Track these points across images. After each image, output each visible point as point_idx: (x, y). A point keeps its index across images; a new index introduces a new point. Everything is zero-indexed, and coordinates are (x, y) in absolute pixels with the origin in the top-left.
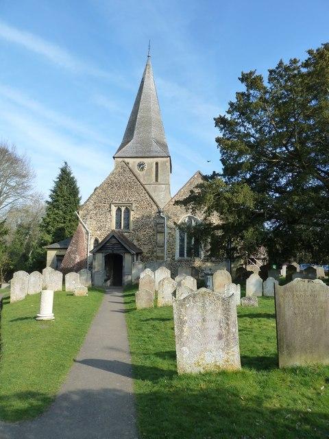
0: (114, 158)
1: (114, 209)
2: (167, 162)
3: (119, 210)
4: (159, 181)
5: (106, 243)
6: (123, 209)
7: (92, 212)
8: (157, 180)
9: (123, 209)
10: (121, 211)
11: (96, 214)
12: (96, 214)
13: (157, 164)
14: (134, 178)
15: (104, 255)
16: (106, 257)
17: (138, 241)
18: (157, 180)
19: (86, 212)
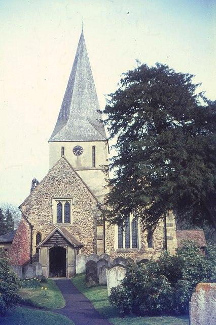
1: (55, 203)
3: (60, 205)
5: (51, 237)
6: (63, 203)
9: (63, 203)
10: (62, 205)
13: (94, 147)
15: (48, 248)
16: (50, 250)
17: (79, 233)
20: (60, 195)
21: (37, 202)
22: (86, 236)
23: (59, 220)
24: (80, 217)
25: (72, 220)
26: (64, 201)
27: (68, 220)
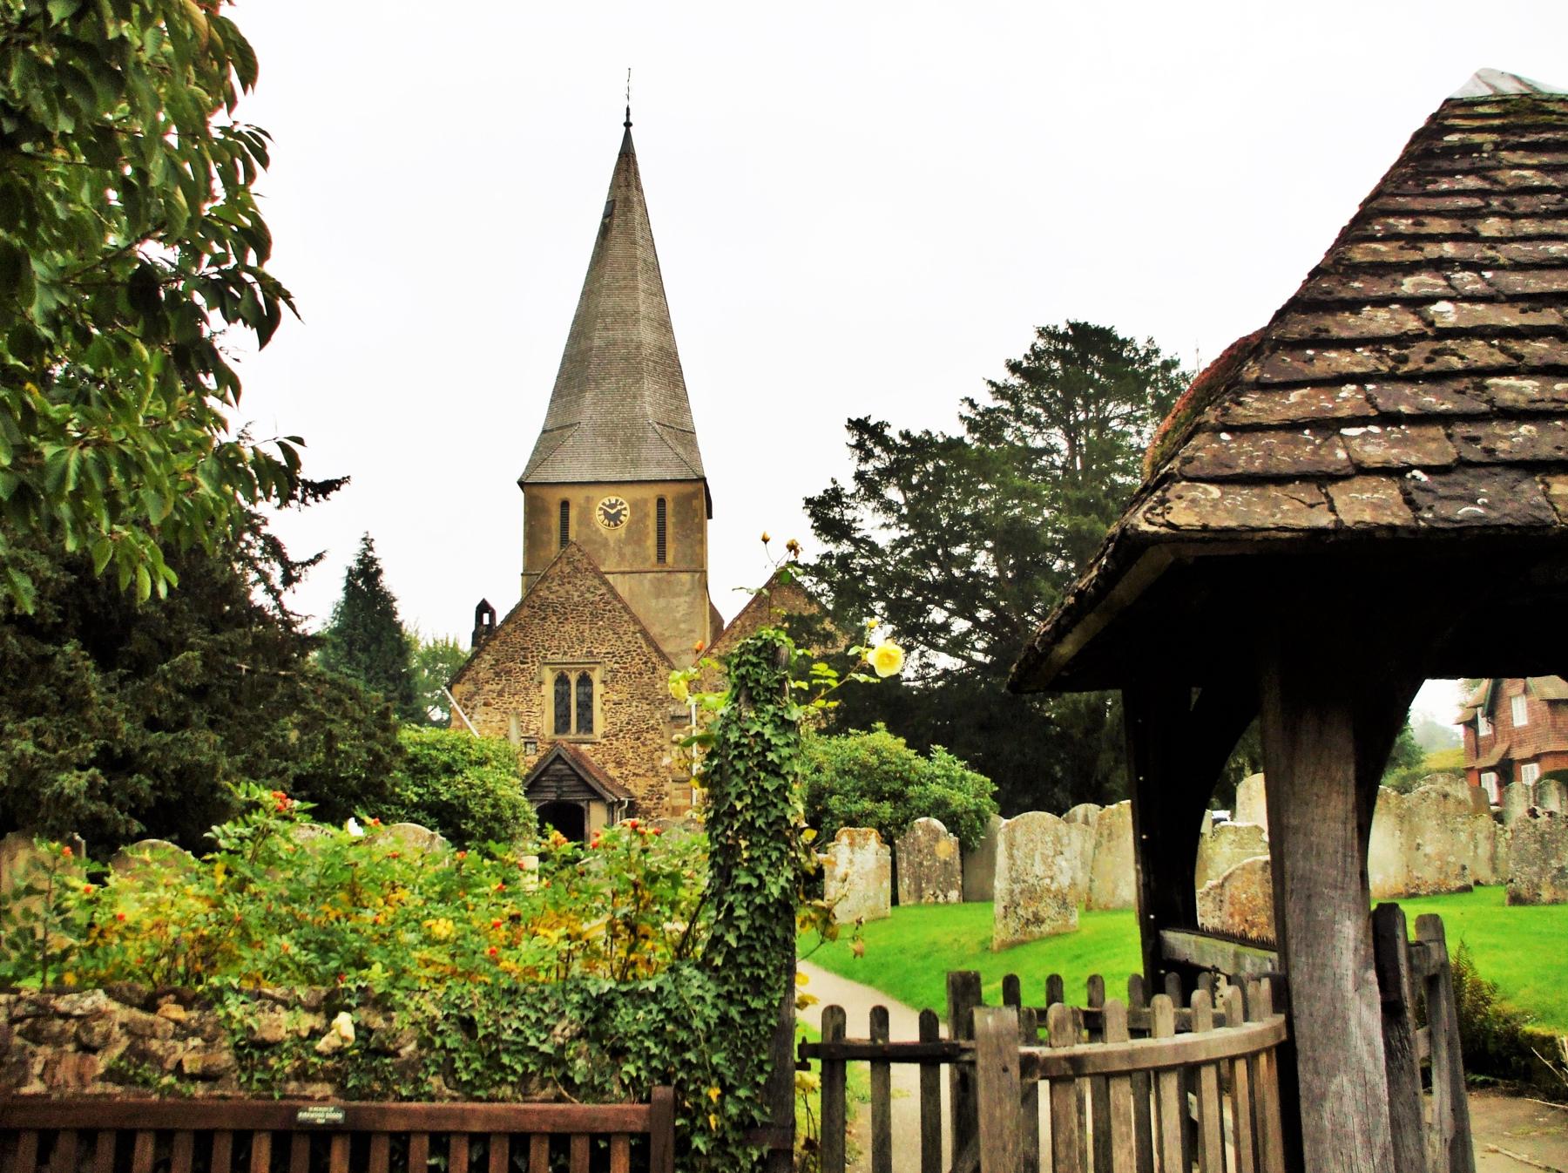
0: (521, 484)
1: (549, 676)
2: (694, 496)
3: (562, 680)
4: (669, 558)
5: (542, 774)
6: (573, 678)
7: (487, 687)
8: (661, 556)
9: (573, 678)
10: (568, 683)
11: (500, 694)
12: (500, 694)
13: (661, 502)
14: (603, 590)
17: (619, 764)
18: (661, 556)
19: (473, 689)
20: (565, 653)
21: (497, 674)
22: (641, 771)
23: (562, 724)
24: (625, 718)
25: (600, 724)
26: (576, 670)
27: (586, 724)
